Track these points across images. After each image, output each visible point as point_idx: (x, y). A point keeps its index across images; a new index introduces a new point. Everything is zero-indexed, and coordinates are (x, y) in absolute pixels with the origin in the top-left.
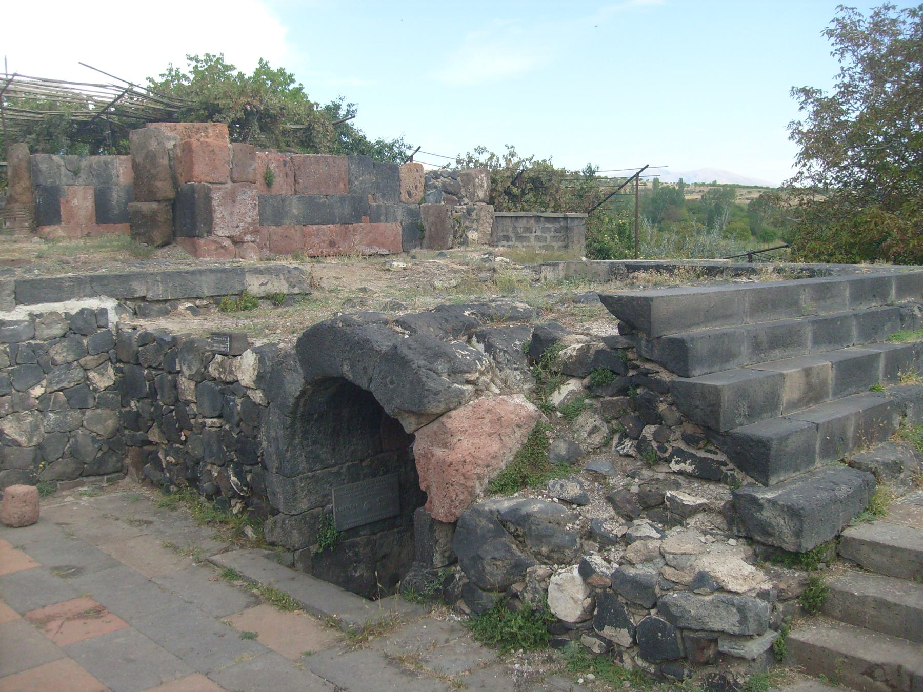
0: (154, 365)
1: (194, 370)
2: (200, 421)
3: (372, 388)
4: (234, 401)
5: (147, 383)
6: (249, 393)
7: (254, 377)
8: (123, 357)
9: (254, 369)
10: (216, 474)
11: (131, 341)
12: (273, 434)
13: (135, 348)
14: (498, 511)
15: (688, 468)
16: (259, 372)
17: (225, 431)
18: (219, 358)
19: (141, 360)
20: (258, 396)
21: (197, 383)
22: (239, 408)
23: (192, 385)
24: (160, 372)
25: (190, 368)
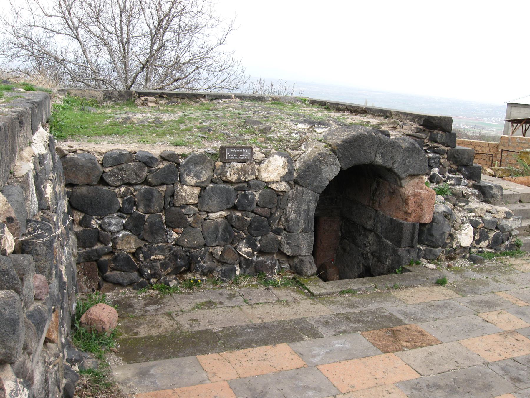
0: (133, 182)
1: (204, 177)
2: (204, 216)
3: (395, 166)
4: (252, 194)
5: (120, 201)
6: (273, 186)
7: (284, 174)
8: (81, 179)
9: (284, 168)
10: (220, 253)
11: (95, 164)
12: (304, 207)
13: (102, 170)
14: (444, 212)
15: (452, 182)
16: (289, 170)
17: (238, 218)
18: (239, 165)
19: (109, 180)
20: (283, 186)
21: (203, 189)
22: (257, 197)
23: (197, 191)
24: (137, 187)
25: (197, 176)
